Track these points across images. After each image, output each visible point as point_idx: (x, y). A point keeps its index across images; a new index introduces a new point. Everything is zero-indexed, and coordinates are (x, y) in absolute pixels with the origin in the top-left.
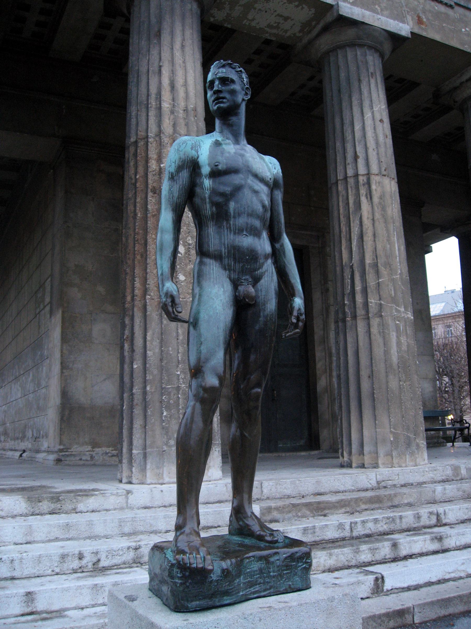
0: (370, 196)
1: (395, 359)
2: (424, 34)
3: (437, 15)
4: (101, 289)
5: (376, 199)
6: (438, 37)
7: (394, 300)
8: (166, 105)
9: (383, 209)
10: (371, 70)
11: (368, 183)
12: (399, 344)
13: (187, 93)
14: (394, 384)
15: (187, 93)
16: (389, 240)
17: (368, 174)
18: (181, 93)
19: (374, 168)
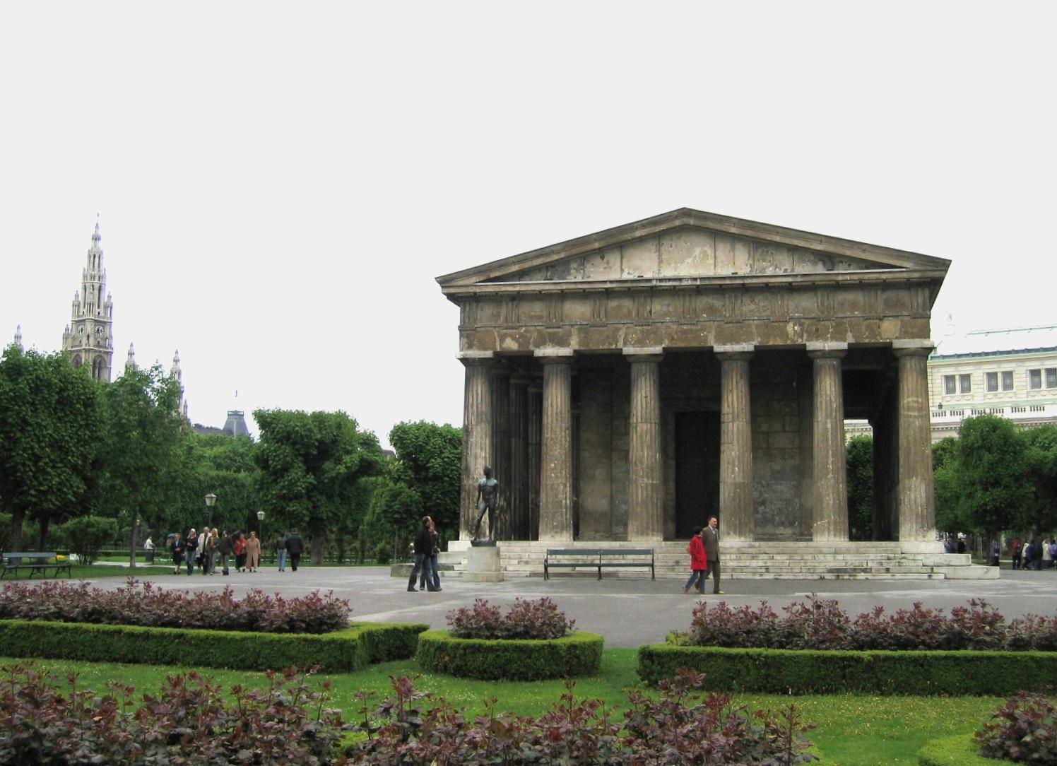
0: (636, 433)
1: (640, 500)
2: (675, 346)
3: (685, 332)
4: (599, 451)
5: (639, 434)
6: (683, 345)
7: (642, 477)
8: (550, 413)
9: (641, 436)
10: (644, 372)
11: (636, 427)
12: (642, 494)
13: (557, 407)
14: (639, 509)
15: (557, 407)
16: (642, 451)
17: (637, 423)
18: (555, 407)
19: (639, 420)
